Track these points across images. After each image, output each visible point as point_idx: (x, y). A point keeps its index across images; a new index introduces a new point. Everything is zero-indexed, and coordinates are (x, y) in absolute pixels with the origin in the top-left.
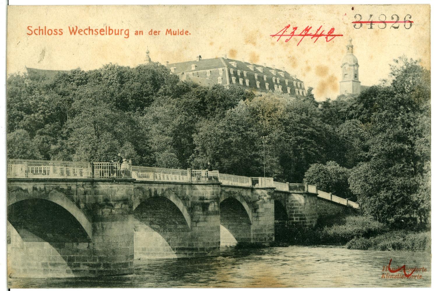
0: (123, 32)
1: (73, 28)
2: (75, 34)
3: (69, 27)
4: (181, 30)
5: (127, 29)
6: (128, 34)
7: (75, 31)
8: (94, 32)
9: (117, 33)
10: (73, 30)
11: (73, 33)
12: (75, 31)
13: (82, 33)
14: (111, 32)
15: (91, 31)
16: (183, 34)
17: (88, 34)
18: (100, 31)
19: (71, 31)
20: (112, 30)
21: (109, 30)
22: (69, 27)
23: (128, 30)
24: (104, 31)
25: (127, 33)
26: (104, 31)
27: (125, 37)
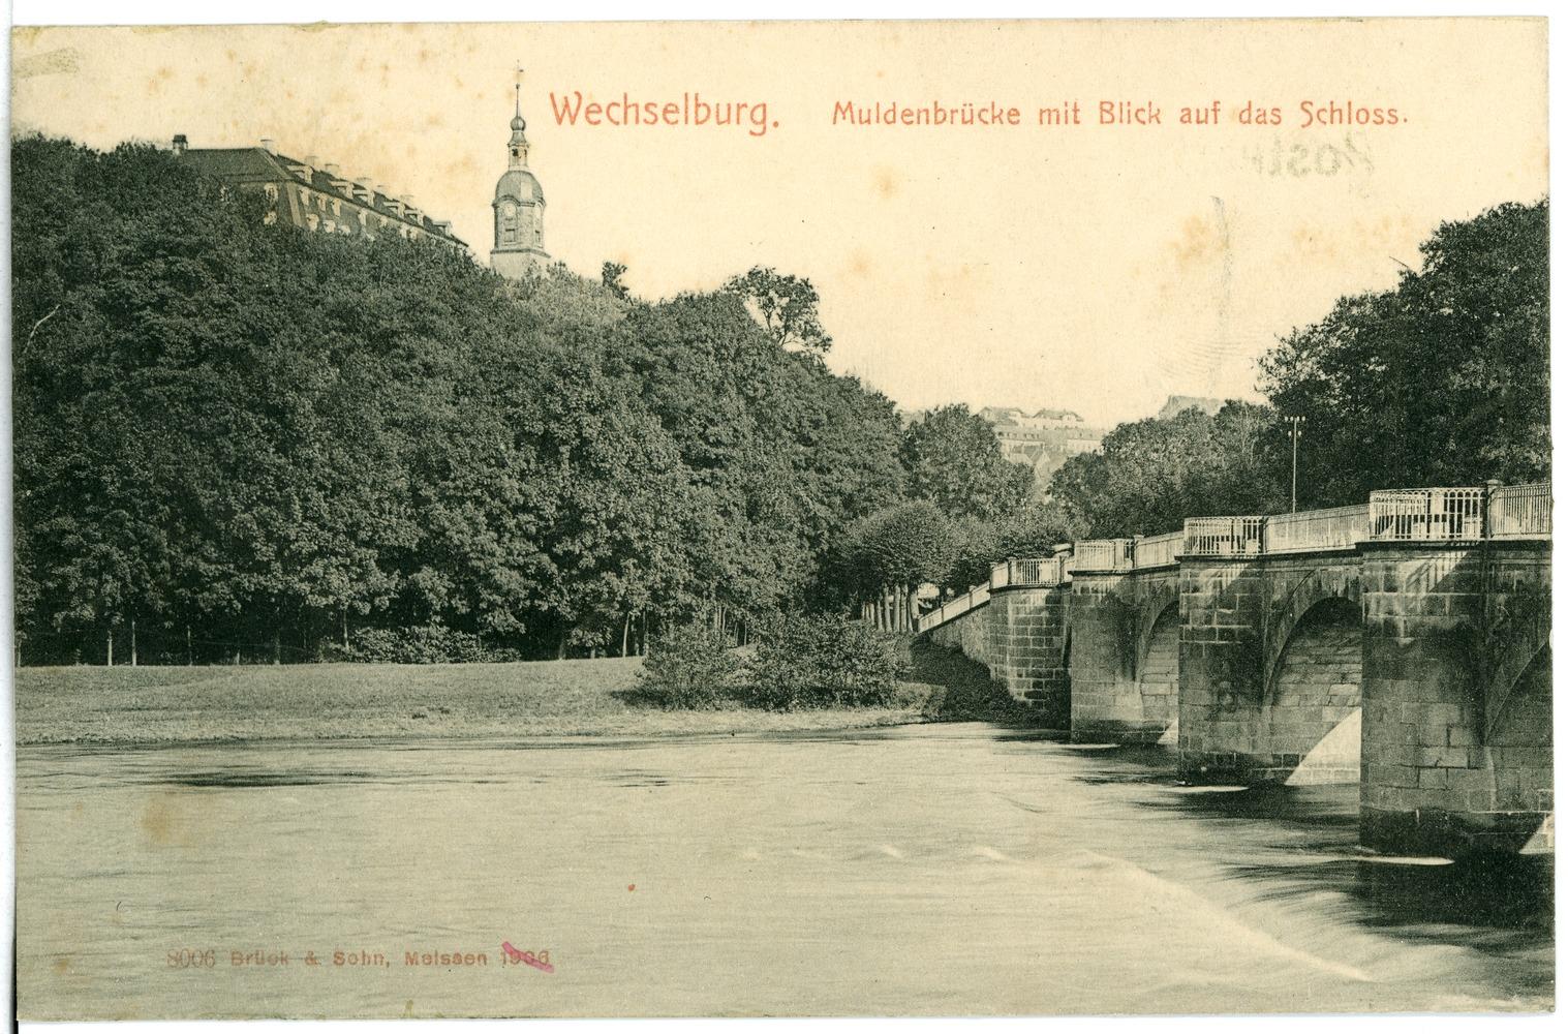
0: (745, 113)
2: (572, 123)
3: (552, 96)
5: (760, 102)
8: (643, 114)
9: (723, 116)
10: (567, 106)
11: (566, 119)
13: (603, 116)
15: (631, 111)
16: (1249, 122)
17: (621, 120)
18: (666, 111)
19: (560, 110)
22: (552, 96)
23: (764, 105)
24: (677, 111)
25: (759, 115)
26: (677, 111)
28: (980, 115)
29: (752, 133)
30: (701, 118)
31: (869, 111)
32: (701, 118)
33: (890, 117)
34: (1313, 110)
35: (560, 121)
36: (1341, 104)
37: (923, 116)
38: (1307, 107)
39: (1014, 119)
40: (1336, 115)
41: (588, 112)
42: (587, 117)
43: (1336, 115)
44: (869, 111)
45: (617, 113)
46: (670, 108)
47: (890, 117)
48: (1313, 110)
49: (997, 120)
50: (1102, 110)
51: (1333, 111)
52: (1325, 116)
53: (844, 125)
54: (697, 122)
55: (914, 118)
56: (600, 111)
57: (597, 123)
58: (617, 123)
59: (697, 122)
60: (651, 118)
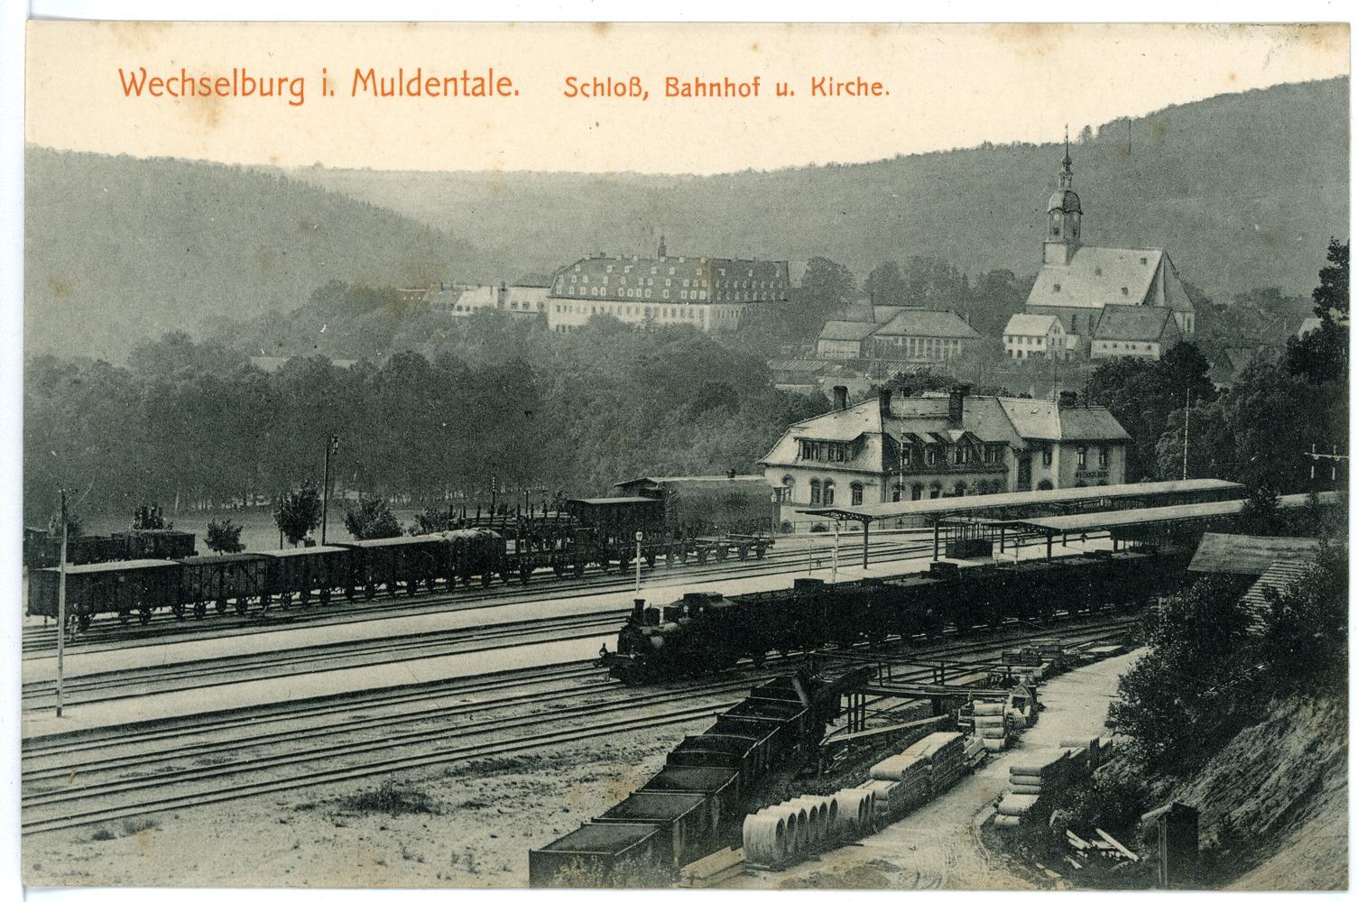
0: (286, 86)
1: (133, 74)
2: (138, 93)
3: (120, 71)
4: (409, 74)
6: (301, 94)
7: (139, 85)
8: (198, 87)
9: (267, 89)
10: (133, 80)
11: (133, 90)
12: (139, 85)
13: (164, 89)
14: (249, 86)
15: (188, 85)
17: (180, 94)
18: (217, 85)
20: (192, 80)
21: (244, 80)
22: (120, 71)
24: (228, 84)
25: (297, 88)
27: (291, 103)
28: (408, 87)
29: (291, 103)
30: (247, 91)
31: (392, 80)
32: (247, 91)
33: (414, 88)
34: (578, 84)
35: (127, 92)
36: (602, 79)
37: (451, 85)
38: (572, 82)
39: (877, 91)
40: (599, 88)
41: (151, 84)
42: (150, 89)
43: (599, 88)
44: (392, 80)
45: (176, 86)
46: (154, 82)
47: (414, 88)
48: (578, 84)
49: (818, 91)
50: (668, 85)
51: (596, 85)
52: (589, 90)
53: (365, 96)
54: (244, 94)
55: (441, 89)
56: (162, 85)
57: (161, 94)
58: (176, 95)
59: (244, 94)
60: (205, 91)
